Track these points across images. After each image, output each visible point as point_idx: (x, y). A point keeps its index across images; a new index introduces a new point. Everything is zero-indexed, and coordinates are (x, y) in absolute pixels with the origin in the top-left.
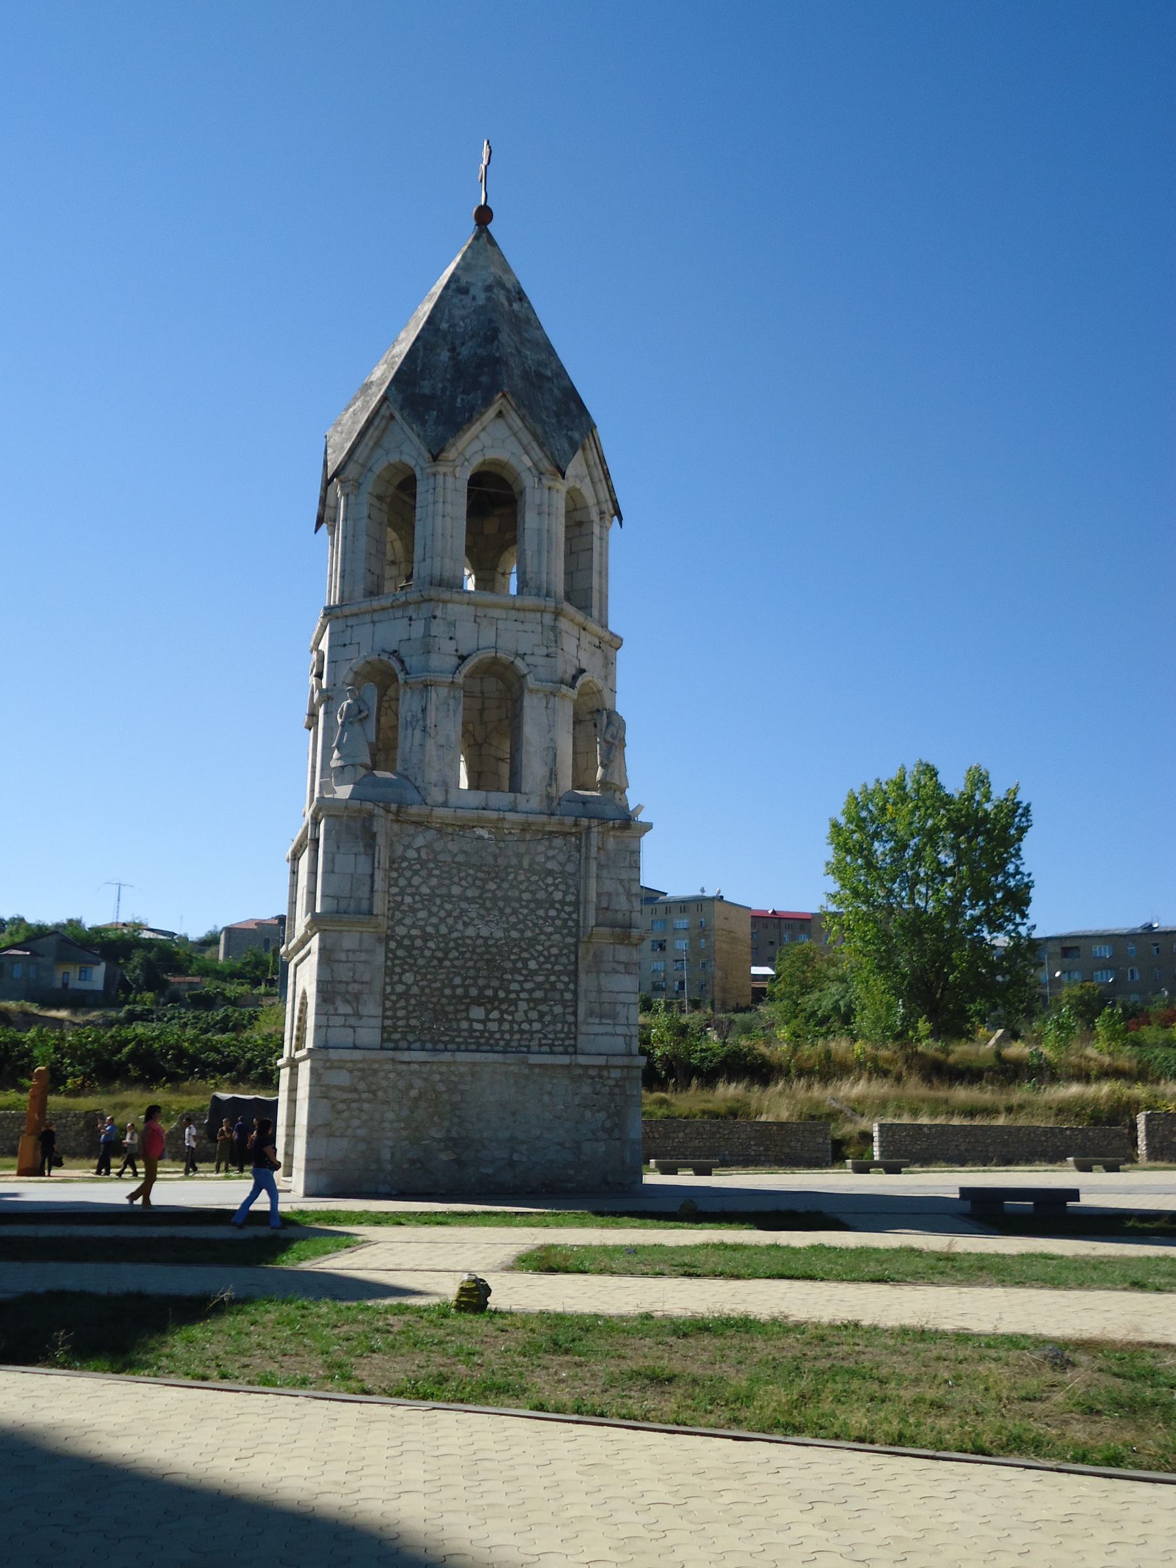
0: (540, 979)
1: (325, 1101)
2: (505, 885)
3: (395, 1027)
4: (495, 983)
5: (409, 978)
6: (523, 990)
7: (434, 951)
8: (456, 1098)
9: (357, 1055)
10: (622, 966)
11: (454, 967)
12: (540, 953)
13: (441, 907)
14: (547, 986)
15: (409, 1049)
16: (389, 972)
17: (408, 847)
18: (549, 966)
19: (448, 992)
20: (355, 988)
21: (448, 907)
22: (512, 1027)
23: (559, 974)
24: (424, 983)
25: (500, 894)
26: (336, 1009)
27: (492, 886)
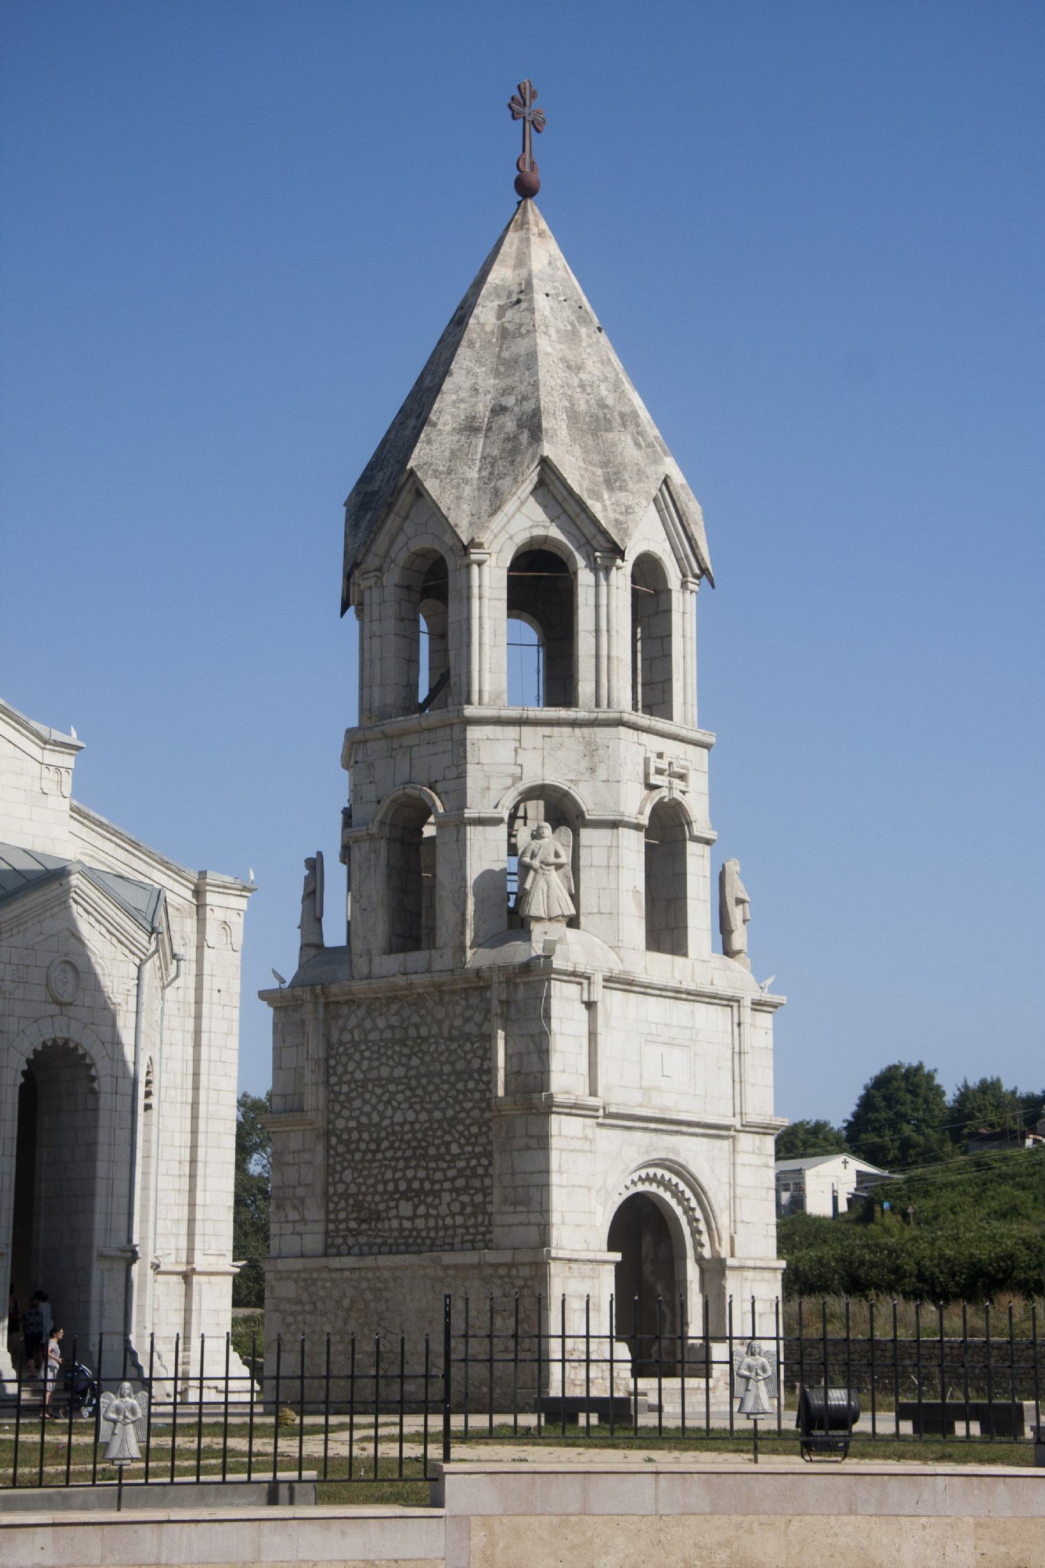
0: (462, 1164)
1: (277, 1314)
2: (427, 1058)
3: (337, 1230)
4: (422, 1174)
5: (348, 1175)
6: (446, 1179)
7: (368, 1143)
8: (381, 1307)
9: (299, 1264)
10: (535, 1140)
11: (385, 1158)
12: (461, 1134)
13: (372, 1093)
14: (468, 1172)
15: (349, 1254)
16: (330, 1171)
17: (343, 1030)
18: (469, 1149)
19: (380, 1188)
20: (300, 1191)
21: (378, 1091)
22: (437, 1223)
23: (477, 1156)
24: (360, 1180)
25: (423, 1070)
26: (286, 1216)
27: (415, 1061)
